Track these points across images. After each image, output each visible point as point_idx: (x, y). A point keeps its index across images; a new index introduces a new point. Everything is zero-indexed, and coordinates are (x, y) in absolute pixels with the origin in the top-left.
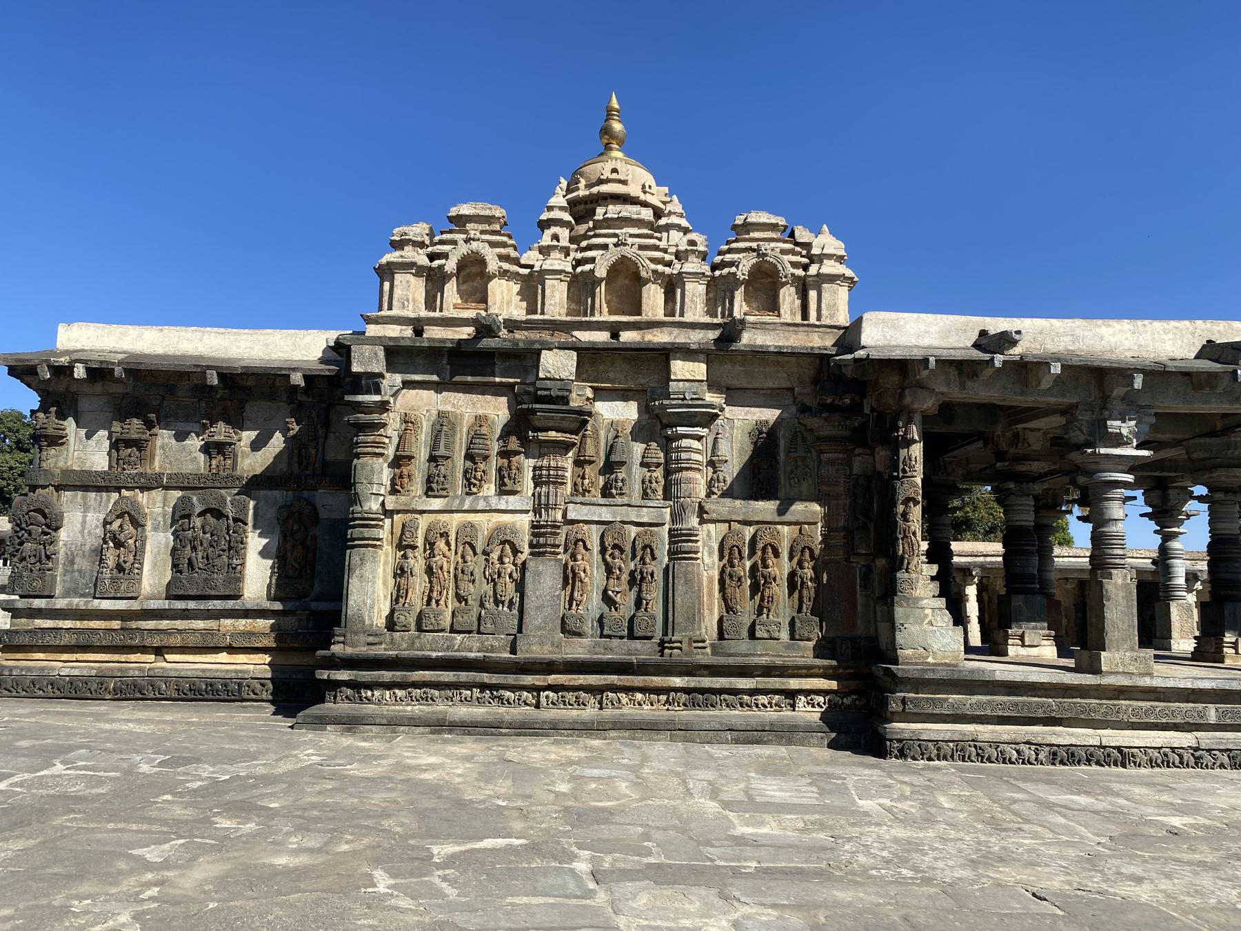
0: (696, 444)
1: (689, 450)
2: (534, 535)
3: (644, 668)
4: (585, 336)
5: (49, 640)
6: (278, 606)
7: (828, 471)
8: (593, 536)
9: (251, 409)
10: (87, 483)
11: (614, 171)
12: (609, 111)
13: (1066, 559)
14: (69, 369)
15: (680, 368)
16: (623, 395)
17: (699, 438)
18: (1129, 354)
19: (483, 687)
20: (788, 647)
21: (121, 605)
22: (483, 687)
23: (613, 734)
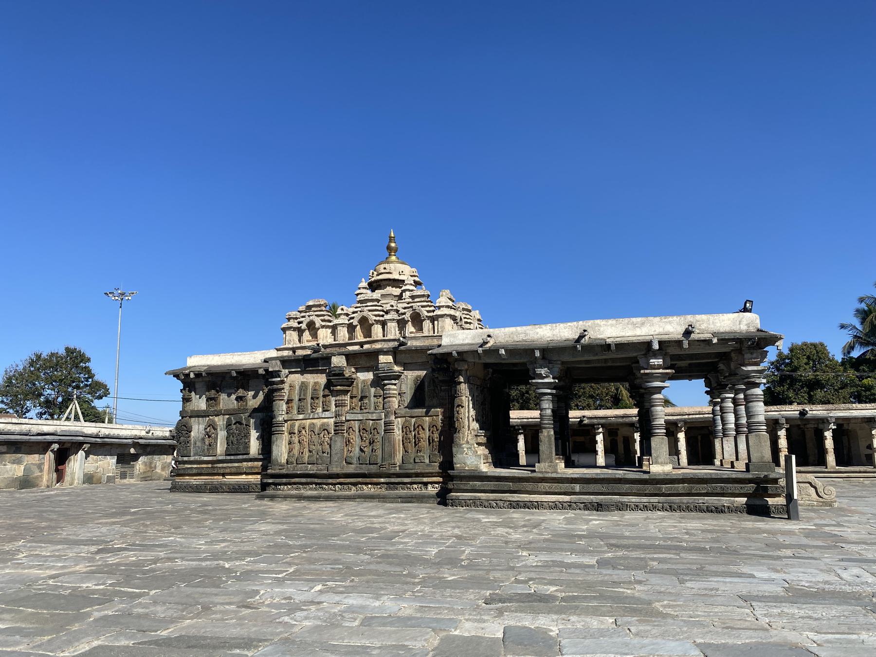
0: (394, 387)
1: (390, 389)
3: (375, 476)
4: (350, 348)
6: (261, 457)
7: (442, 394)
8: (356, 425)
9: (251, 383)
12: (390, 237)
14: (188, 375)
15: (383, 359)
16: (367, 369)
17: (395, 384)
19: (316, 484)
20: (428, 465)
21: (210, 458)
22: (316, 484)
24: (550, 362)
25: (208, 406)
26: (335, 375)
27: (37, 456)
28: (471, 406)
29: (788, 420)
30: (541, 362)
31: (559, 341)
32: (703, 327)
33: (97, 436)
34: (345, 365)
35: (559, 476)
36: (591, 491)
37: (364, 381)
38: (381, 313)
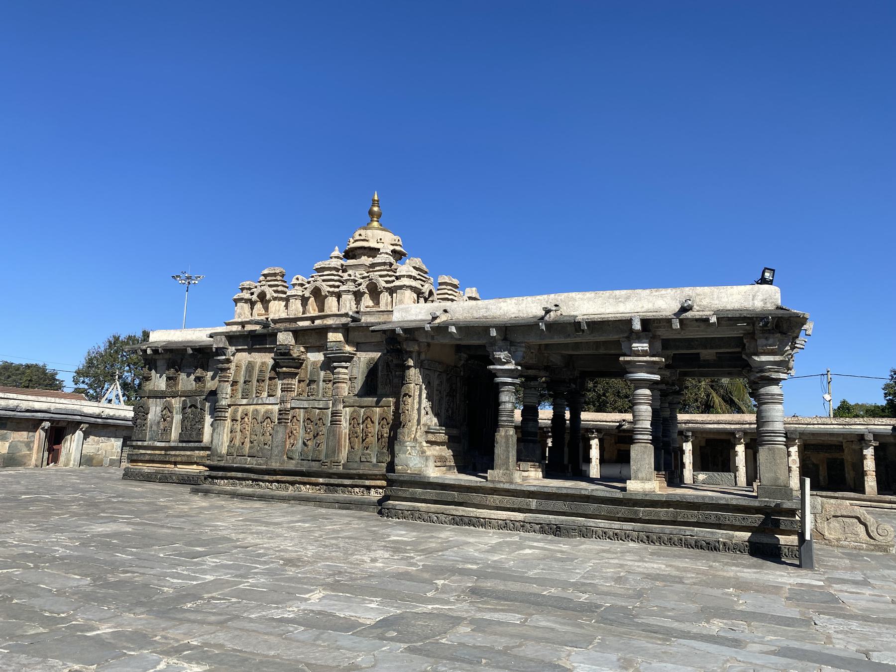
0: (346, 371)
1: (339, 373)
2: (280, 414)
4: (301, 324)
5: (142, 458)
8: (301, 414)
10: (158, 395)
11: (360, 235)
13: (816, 426)
14: (145, 351)
15: (332, 337)
17: (346, 368)
18: (513, 316)
19: (253, 480)
20: (374, 465)
21: (163, 444)
23: (292, 502)
24: (512, 344)
25: (167, 385)
26: (281, 354)
27: (25, 433)
28: (424, 395)
29: (877, 436)
30: (500, 343)
31: (523, 319)
32: (704, 303)
33: (99, 416)
34: (293, 342)
35: (512, 487)
36: (550, 509)
37: (314, 363)
38: (337, 283)
